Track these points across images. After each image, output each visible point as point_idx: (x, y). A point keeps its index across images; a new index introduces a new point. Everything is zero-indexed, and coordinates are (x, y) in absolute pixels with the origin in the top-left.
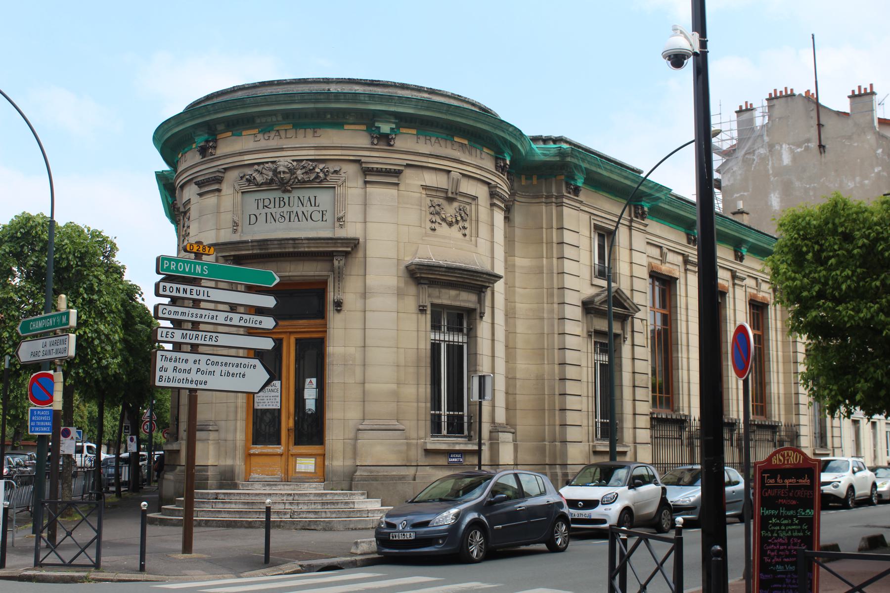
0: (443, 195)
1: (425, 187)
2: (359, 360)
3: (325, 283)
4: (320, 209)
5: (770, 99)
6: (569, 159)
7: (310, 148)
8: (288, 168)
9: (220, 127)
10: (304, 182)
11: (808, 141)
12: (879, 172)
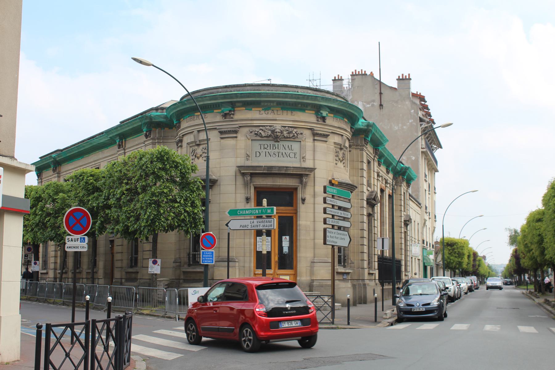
0: (339, 147)
1: (335, 143)
2: (312, 228)
3: (296, 189)
4: (294, 152)
5: (352, 75)
6: (370, 128)
7: (290, 121)
8: (281, 131)
9: (237, 104)
10: (287, 138)
11: (374, 101)
12: (412, 123)
